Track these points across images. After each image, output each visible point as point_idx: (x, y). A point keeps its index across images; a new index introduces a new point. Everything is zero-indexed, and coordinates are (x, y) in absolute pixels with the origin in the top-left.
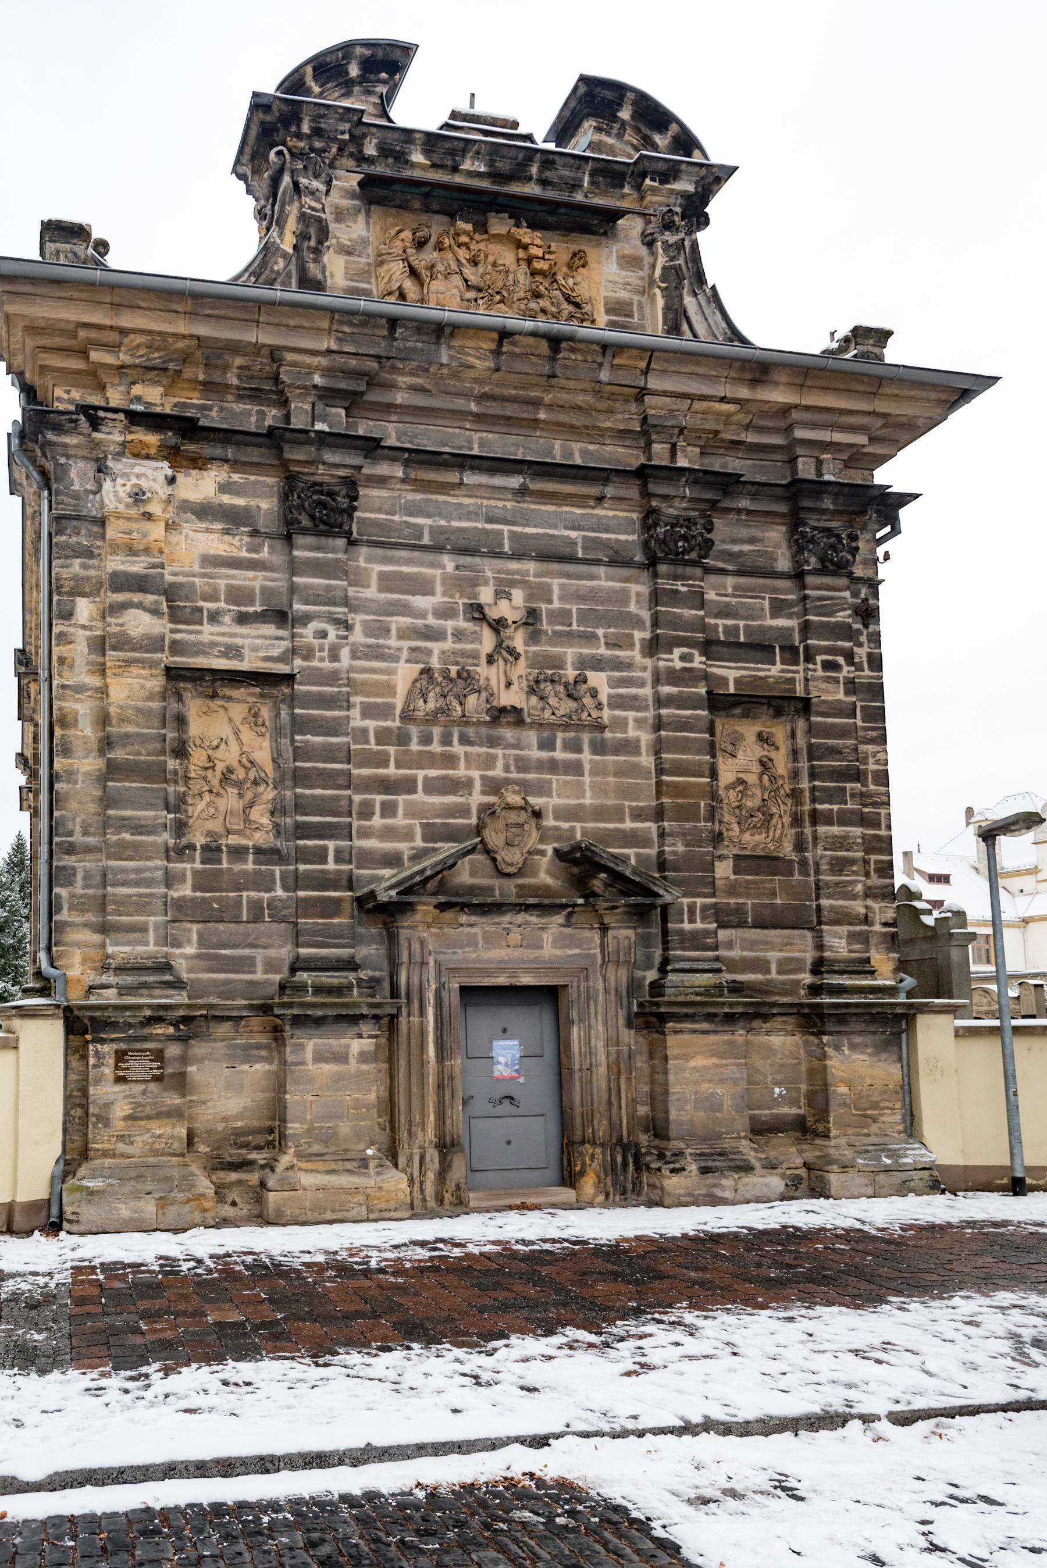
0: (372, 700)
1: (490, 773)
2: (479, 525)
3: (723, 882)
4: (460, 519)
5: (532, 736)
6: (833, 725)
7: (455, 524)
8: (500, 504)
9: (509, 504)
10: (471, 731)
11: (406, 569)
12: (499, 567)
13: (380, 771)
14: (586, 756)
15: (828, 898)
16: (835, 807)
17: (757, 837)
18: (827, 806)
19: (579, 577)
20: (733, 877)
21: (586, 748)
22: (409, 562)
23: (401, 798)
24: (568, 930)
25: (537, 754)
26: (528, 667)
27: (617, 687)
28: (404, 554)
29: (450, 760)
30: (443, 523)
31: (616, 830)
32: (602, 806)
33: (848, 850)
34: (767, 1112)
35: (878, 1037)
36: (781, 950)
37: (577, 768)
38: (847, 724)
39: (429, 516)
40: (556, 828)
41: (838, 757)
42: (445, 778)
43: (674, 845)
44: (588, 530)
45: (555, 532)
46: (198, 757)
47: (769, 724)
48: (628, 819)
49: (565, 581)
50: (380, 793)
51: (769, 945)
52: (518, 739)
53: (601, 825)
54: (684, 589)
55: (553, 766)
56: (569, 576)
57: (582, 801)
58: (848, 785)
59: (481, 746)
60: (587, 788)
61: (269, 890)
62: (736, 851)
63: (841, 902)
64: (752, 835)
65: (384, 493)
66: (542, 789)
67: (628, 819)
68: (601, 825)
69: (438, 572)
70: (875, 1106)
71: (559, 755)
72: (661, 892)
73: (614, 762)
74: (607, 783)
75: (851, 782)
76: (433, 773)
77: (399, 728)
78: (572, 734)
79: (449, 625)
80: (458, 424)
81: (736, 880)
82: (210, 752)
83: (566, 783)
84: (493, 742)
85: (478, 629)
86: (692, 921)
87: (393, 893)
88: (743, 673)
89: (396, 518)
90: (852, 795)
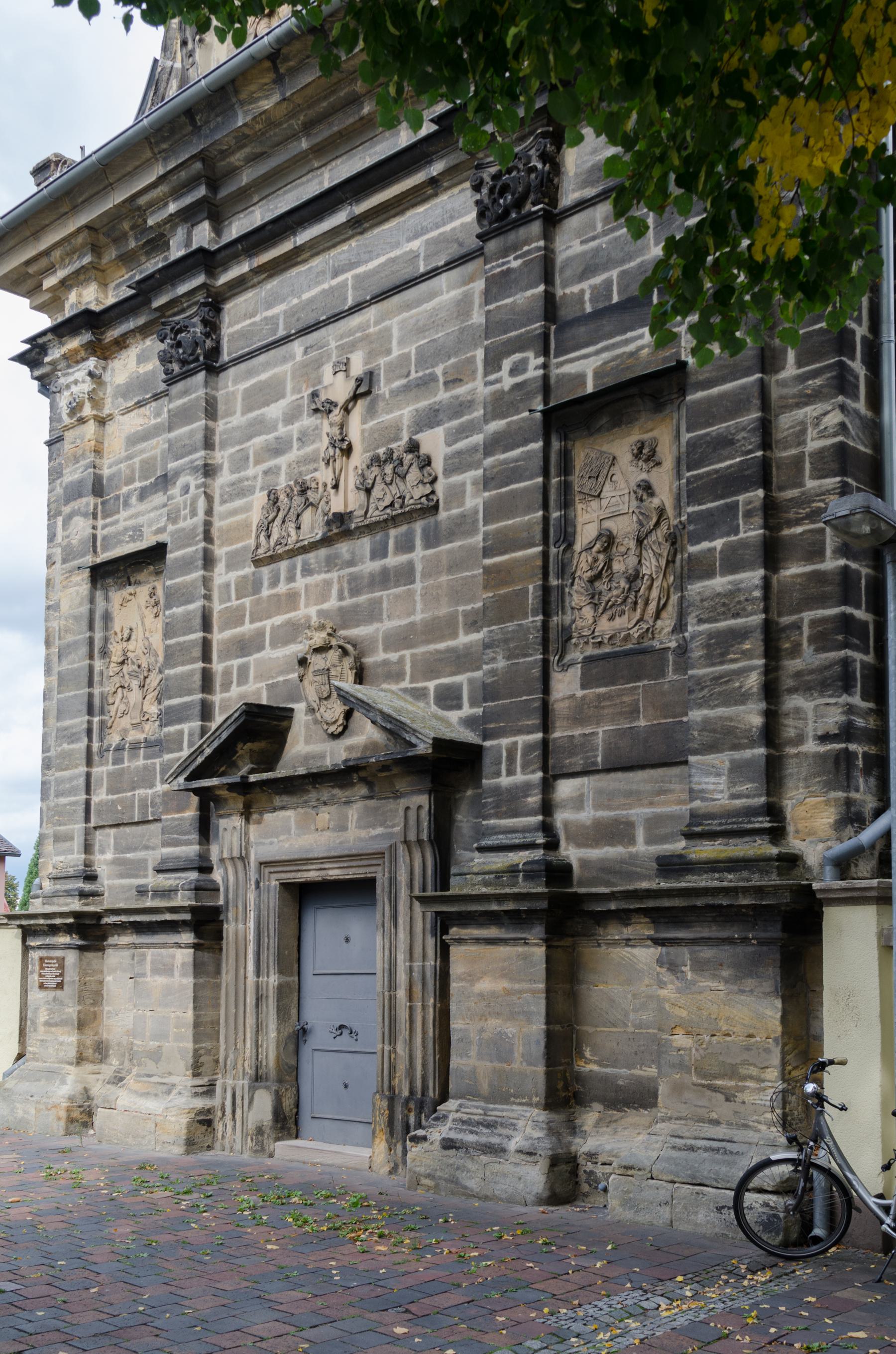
0: (234, 547)
1: (326, 606)
2: (326, 286)
3: (566, 703)
4: (309, 288)
5: (365, 544)
6: (722, 396)
7: (306, 296)
8: (345, 247)
9: (353, 243)
10: (311, 556)
11: (263, 377)
12: (341, 332)
13: (238, 630)
14: (419, 554)
15: (700, 706)
16: (718, 543)
17: (619, 622)
18: (705, 545)
19: (419, 302)
20: (580, 693)
21: (418, 542)
22: (266, 366)
23: (251, 659)
24: (372, 803)
25: (370, 566)
26: (366, 451)
27: (456, 441)
28: (262, 358)
29: (292, 599)
30: (295, 301)
31: (449, 650)
32: (434, 619)
33: (736, 615)
34: (624, 1071)
35: (740, 949)
36: (651, 804)
37: (406, 574)
38: (743, 388)
39: (283, 300)
40: (386, 663)
41: (725, 452)
42: (288, 623)
43: (493, 660)
44: (432, 230)
45: (397, 252)
46: (116, 650)
47: (650, 425)
48: (461, 631)
49: (405, 315)
50: (238, 657)
51: (634, 797)
52: (353, 553)
53: (432, 647)
54: (515, 264)
55: (384, 579)
56: (408, 307)
57: (412, 619)
58: (741, 498)
59: (319, 572)
60: (418, 598)
61: (151, 787)
62: (590, 651)
63: (721, 711)
64: (612, 618)
65: (249, 295)
66: (373, 613)
67: (461, 631)
68: (432, 647)
69: (288, 367)
70: (732, 1072)
71: (393, 560)
72: (414, 740)
73: (450, 552)
74: (439, 586)
75: (746, 490)
76: (278, 620)
77: (254, 574)
78: (404, 528)
79: (295, 428)
80: (307, 168)
81: (583, 698)
82: (125, 644)
83: (397, 597)
84: (330, 564)
85: (319, 421)
86: (510, 772)
87: (181, 780)
88: (606, 356)
89: (258, 318)
90: (748, 514)
